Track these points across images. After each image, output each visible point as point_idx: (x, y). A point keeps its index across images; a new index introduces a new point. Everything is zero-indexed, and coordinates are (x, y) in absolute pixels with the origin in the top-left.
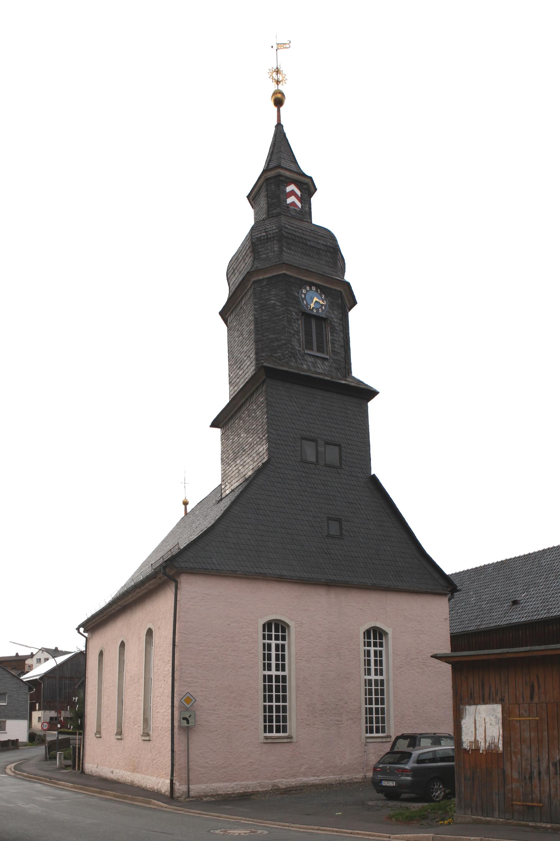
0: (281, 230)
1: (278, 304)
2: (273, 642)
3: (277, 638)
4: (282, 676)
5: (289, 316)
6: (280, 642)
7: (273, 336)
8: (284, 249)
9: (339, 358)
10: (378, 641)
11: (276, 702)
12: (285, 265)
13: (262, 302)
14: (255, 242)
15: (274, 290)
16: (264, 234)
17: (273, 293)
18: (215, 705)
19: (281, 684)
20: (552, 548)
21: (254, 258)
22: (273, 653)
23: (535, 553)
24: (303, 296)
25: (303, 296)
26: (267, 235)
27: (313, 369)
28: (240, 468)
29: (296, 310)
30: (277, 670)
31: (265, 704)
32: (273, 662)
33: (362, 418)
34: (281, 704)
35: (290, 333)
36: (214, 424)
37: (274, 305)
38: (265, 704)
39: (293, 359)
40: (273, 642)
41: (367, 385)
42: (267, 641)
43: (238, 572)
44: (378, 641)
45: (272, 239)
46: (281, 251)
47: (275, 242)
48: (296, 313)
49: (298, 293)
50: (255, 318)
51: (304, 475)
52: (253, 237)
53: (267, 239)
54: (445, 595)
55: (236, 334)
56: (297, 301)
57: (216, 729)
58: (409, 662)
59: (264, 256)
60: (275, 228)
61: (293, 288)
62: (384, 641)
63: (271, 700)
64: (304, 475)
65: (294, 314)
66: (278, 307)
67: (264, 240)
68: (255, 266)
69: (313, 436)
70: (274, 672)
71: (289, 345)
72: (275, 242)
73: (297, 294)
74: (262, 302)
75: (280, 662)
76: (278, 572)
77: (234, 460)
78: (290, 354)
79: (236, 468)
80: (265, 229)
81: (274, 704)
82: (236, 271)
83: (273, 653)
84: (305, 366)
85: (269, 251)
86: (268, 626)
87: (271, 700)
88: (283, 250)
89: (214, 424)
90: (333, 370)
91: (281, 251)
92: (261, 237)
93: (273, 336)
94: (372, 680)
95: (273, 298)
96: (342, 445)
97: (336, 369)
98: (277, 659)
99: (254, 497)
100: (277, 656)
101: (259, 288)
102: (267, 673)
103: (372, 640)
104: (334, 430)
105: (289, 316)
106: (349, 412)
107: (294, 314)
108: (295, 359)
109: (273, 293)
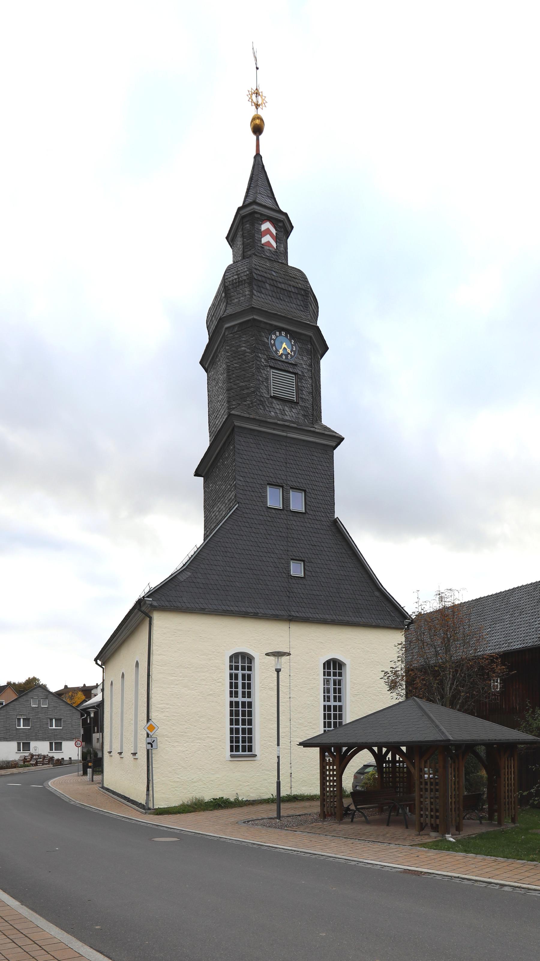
0: (251, 273)
1: (249, 351)
2: (240, 673)
3: (243, 669)
4: (235, 702)
5: (258, 363)
6: (246, 672)
7: (243, 384)
8: (255, 292)
9: (307, 405)
10: (337, 671)
11: (242, 725)
12: (253, 310)
13: (233, 349)
14: (229, 287)
15: (244, 336)
16: (236, 277)
17: (244, 339)
18: (186, 728)
19: (247, 709)
20: (521, 587)
21: (227, 303)
22: (240, 681)
23: (506, 591)
24: (273, 342)
25: (273, 342)
26: (239, 278)
27: (280, 416)
28: (217, 514)
29: (265, 356)
30: (244, 696)
31: (232, 726)
32: (240, 690)
33: (328, 465)
34: (247, 727)
35: (259, 380)
36: (197, 474)
37: (245, 351)
38: (232, 726)
39: (261, 407)
40: (240, 673)
41: (333, 432)
42: (234, 671)
43: (206, 610)
44: (337, 671)
45: (243, 282)
46: (252, 294)
47: (246, 285)
48: (265, 359)
49: (268, 339)
50: (228, 366)
51: (269, 519)
52: (226, 281)
53: (239, 282)
54: (402, 629)
55: (214, 383)
56: (267, 347)
57: (186, 749)
58: (366, 690)
59: (236, 300)
60: (246, 269)
61: (263, 334)
62: (343, 671)
63: (237, 723)
64: (269, 519)
65: (263, 360)
66: (247, 354)
67: (236, 283)
68: (227, 311)
69: (279, 482)
70: (240, 699)
71: (258, 393)
72: (246, 285)
73: (266, 341)
74: (233, 349)
75: (246, 690)
76: (243, 609)
77: (213, 507)
78: (258, 402)
79: (214, 514)
80: (237, 272)
81: (240, 727)
82: (214, 318)
83: (240, 681)
84: (273, 413)
85: (241, 295)
86: (234, 657)
87: (237, 723)
88: (253, 294)
89: (197, 474)
90: (301, 417)
91: (252, 294)
92: (233, 280)
93: (243, 384)
94: (239, 702)
95: (244, 345)
96: (307, 490)
97: (304, 416)
98: (243, 687)
99: (221, 540)
100: (243, 684)
101: (232, 335)
102: (234, 699)
103: (332, 671)
104: (300, 476)
105: (258, 363)
106: (315, 458)
107: (263, 360)
108: (264, 406)
109: (244, 339)
